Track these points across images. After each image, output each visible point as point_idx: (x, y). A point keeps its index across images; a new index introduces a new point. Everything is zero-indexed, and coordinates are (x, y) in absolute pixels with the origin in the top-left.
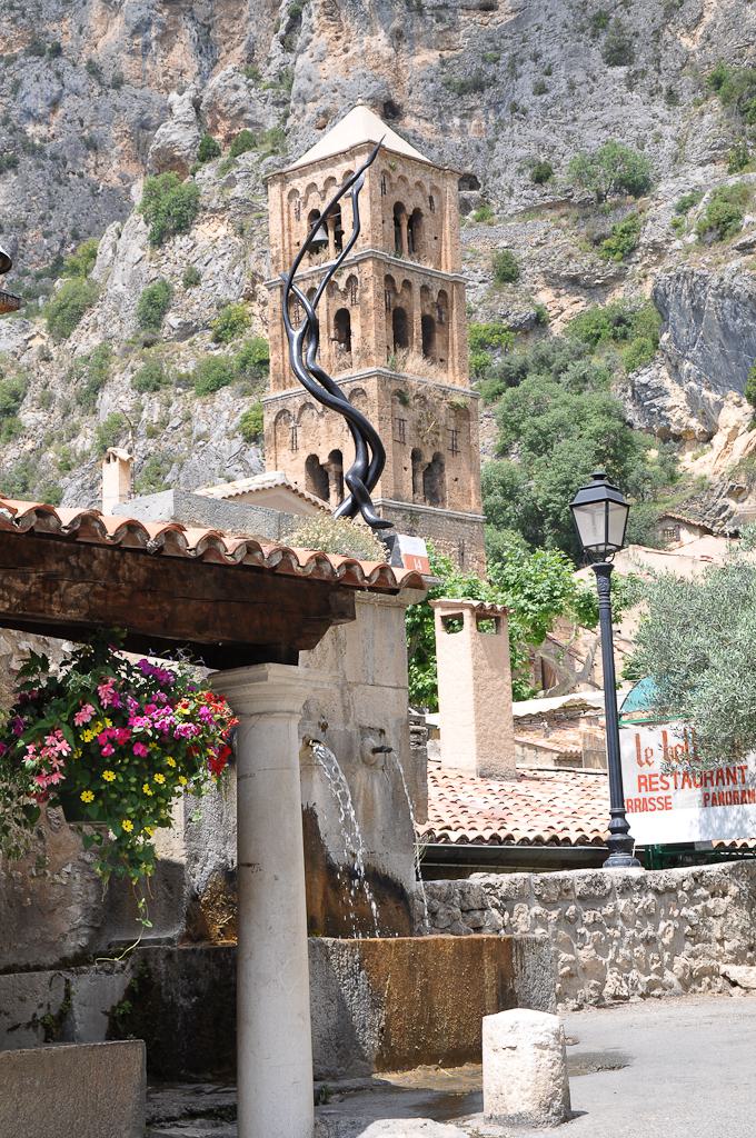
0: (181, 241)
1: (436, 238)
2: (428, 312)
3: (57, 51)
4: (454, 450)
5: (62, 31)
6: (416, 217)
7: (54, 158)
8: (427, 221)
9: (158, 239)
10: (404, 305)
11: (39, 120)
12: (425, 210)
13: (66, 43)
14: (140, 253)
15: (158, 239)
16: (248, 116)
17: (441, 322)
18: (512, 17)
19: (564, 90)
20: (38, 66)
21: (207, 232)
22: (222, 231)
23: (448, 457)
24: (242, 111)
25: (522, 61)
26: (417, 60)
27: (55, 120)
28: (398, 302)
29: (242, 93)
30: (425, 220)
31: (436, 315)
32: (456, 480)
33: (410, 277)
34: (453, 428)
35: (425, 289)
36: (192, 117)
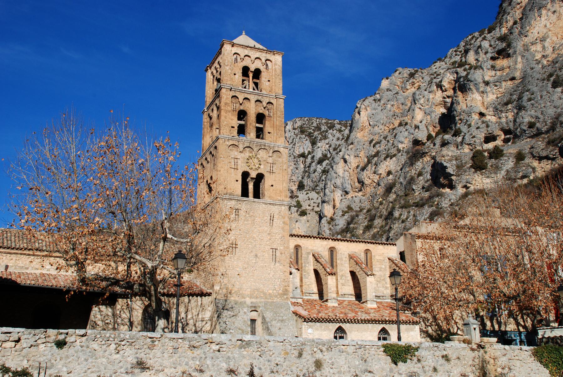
1: (269, 81)
2: (261, 112)
4: (271, 172)
6: (257, 73)
8: (264, 76)
10: (245, 109)
12: (262, 68)
13: (409, 122)
18: (521, 80)
19: (539, 98)
23: (267, 175)
25: (524, 93)
26: (489, 99)
28: (242, 108)
30: (263, 74)
31: (266, 113)
32: (272, 186)
33: (248, 96)
34: (271, 162)
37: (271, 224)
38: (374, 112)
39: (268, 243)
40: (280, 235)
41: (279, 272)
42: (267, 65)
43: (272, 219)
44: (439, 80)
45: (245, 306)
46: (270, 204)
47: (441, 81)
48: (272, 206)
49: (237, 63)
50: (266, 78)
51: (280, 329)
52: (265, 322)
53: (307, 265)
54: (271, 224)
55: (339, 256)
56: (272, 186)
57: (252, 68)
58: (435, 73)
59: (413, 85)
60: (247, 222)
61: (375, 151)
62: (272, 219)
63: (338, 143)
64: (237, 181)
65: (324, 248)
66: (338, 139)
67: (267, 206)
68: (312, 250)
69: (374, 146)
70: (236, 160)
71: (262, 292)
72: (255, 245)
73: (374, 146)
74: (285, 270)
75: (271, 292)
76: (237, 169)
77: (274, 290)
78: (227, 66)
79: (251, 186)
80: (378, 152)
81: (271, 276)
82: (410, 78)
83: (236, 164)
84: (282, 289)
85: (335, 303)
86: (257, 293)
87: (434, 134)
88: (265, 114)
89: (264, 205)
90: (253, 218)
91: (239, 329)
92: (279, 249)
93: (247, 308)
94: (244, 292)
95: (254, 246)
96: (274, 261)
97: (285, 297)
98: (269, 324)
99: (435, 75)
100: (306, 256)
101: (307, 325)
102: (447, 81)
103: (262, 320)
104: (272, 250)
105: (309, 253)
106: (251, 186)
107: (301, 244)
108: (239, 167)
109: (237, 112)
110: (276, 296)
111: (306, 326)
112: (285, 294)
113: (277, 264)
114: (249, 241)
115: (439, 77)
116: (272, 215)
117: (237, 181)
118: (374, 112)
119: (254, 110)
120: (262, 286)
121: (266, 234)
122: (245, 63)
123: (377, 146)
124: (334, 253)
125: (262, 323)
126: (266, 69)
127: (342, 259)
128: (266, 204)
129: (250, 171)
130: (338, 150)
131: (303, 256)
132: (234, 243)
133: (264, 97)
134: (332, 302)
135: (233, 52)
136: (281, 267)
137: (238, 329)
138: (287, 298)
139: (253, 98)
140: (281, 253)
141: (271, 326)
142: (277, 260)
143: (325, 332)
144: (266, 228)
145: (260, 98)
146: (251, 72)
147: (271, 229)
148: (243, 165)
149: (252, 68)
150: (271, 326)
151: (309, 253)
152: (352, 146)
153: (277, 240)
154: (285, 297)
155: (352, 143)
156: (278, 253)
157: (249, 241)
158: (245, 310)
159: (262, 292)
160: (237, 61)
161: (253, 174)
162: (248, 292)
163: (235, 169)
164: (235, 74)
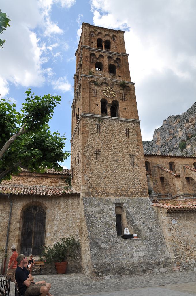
0: (185, 150)
3: (176, 137)
5: (176, 135)
7: (177, 148)
9: (182, 150)
10: (101, 61)
11: (175, 145)
12: (111, 40)
13: (177, 136)
14: (180, 153)
15: (182, 150)
16: (193, 134)
17: (119, 66)
20: (174, 139)
21: (188, 147)
22: (190, 147)
24: (192, 133)
27: (176, 145)
28: (98, 61)
29: (192, 131)
31: (117, 65)
32: (125, 109)
33: (103, 54)
35: (109, 58)
36: (185, 135)
37: (127, 136)
38: (162, 134)
39: (126, 150)
40: (136, 144)
41: (137, 173)
42: (114, 39)
43: (127, 132)
44: (187, 119)
45: (110, 202)
46: (125, 121)
47: (188, 119)
48: (127, 123)
49: (93, 36)
50: (114, 45)
51: (144, 222)
52: (129, 216)
53: (155, 175)
54: (127, 136)
55: (176, 168)
56: (125, 109)
57: (104, 39)
58: (185, 116)
59: (176, 122)
60: (107, 134)
61: (164, 149)
62: (127, 132)
63: (148, 148)
64: (97, 105)
65: (166, 163)
66: (148, 146)
67: (122, 122)
68: (157, 165)
69: (163, 147)
70: (96, 91)
71: (123, 191)
72: (115, 152)
73: (163, 147)
74: (142, 171)
75: (132, 190)
76: (97, 97)
77: (134, 189)
78: (86, 36)
79: (109, 110)
80: (165, 149)
81: (131, 177)
82: (175, 119)
83: (96, 93)
84: (141, 187)
85: (183, 199)
86: (120, 191)
87: (190, 137)
88: (115, 65)
89: (120, 122)
90: (112, 132)
91: (106, 224)
92: (135, 154)
93: (111, 205)
94: (108, 191)
95: (114, 153)
96: (132, 164)
97: (145, 194)
98: (133, 218)
99: (185, 117)
100: (153, 169)
101: (170, 216)
102: (190, 119)
103: (127, 214)
104: (130, 156)
105: (155, 167)
106: (109, 110)
107: (149, 161)
108: (98, 96)
109: (95, 63)
110: (137, 194)
111: (170, 217)
112: (144, 192)
113: (135, 167)
114: (110, 149)
115: (187, 117)
116: (127, 129)
117: (97, 105)
118: (162, 134)
119: (107, 62)
120: (124, 185)
121: (124, 144)
122: (98, 37)
123: (165, 147)
124: (173, 166)
125: (127, 217)
126: (114, 40)
127: (179, 170)
128: (122, 121)
129: (107, 99)
130: (149, 151)
131: (151, 169)
132: (98, 150)
133: (113, 55)
134: (181, 199)
135: (91, 30)
136: (139, 169)
137: (104, 224)
138: (146, 195)
139: (106, 56)
140: (138, 159)
141: (135, 219)
142: (135, 164)
143: (188, 222)
144: (123, 139)
145: (111, 55)
146: (104, 42)
147: (127, 140)
148: (101, 94)
149: (104, 39)
150: (135, 219)
151: (155, 167)
152: (154, 148)
153: (133, 148)
154: (145, 194)
155: (154, 147)
156: (135, 159)
157: (110, 149)
158: (110, 207)
159: (123, 191)
160: (93, 36)
161: (110, 101)
162: (112, 191)
163: (95, 97)
164: (92, 43)
